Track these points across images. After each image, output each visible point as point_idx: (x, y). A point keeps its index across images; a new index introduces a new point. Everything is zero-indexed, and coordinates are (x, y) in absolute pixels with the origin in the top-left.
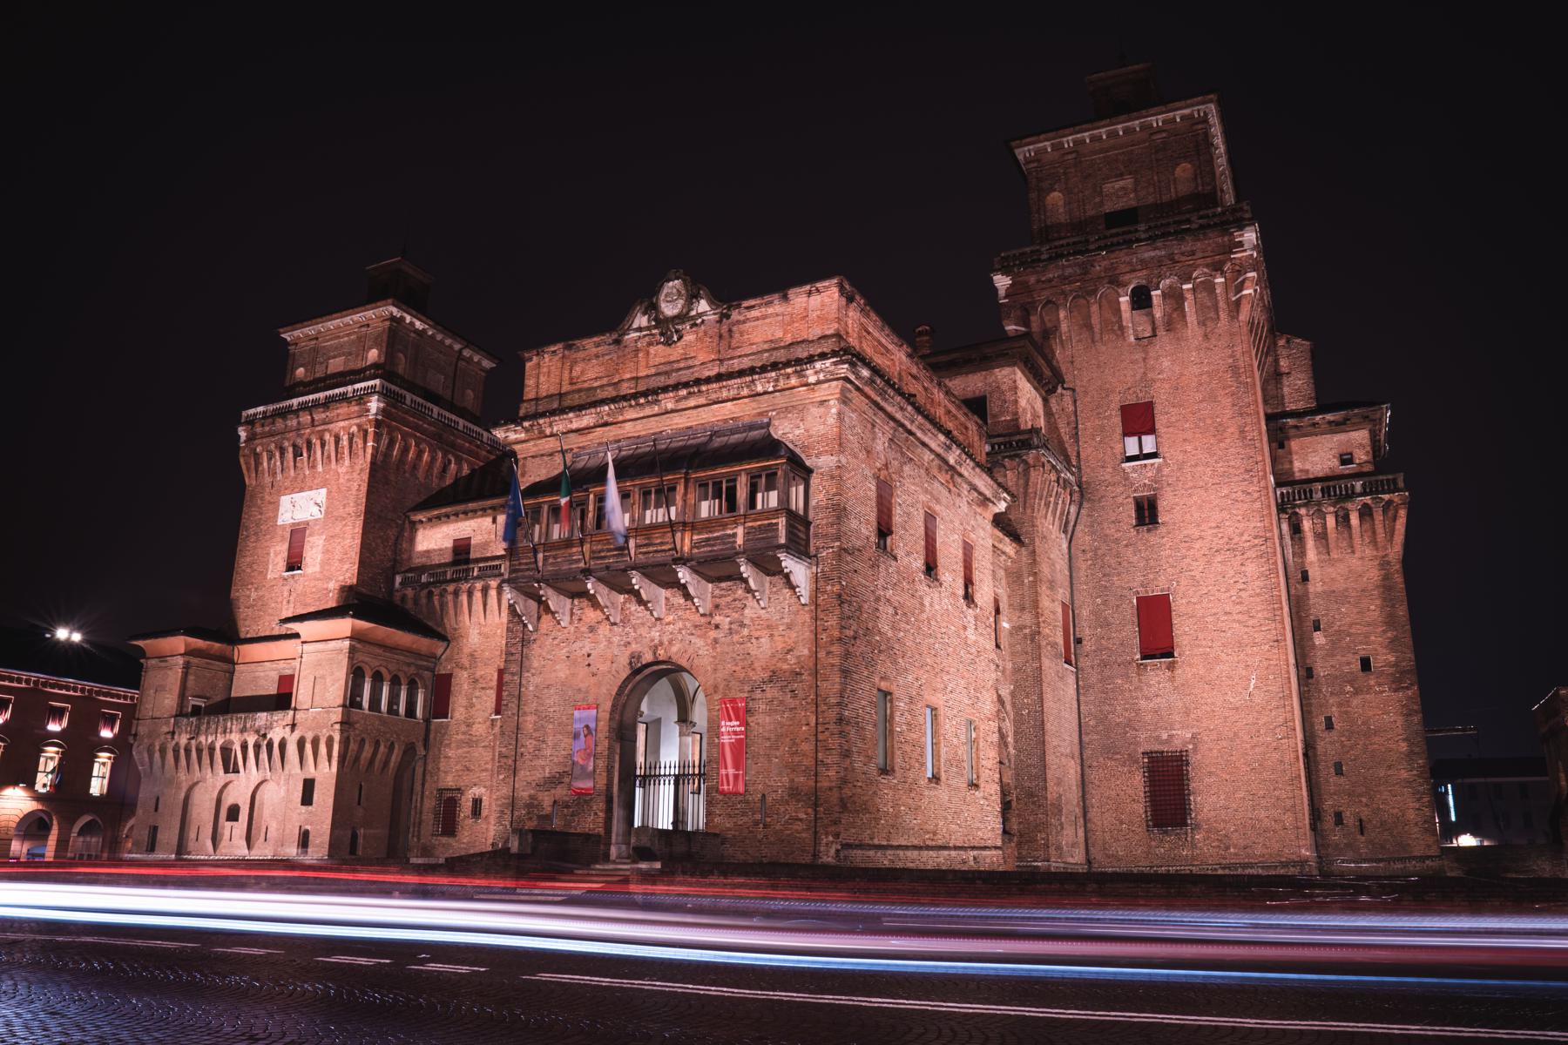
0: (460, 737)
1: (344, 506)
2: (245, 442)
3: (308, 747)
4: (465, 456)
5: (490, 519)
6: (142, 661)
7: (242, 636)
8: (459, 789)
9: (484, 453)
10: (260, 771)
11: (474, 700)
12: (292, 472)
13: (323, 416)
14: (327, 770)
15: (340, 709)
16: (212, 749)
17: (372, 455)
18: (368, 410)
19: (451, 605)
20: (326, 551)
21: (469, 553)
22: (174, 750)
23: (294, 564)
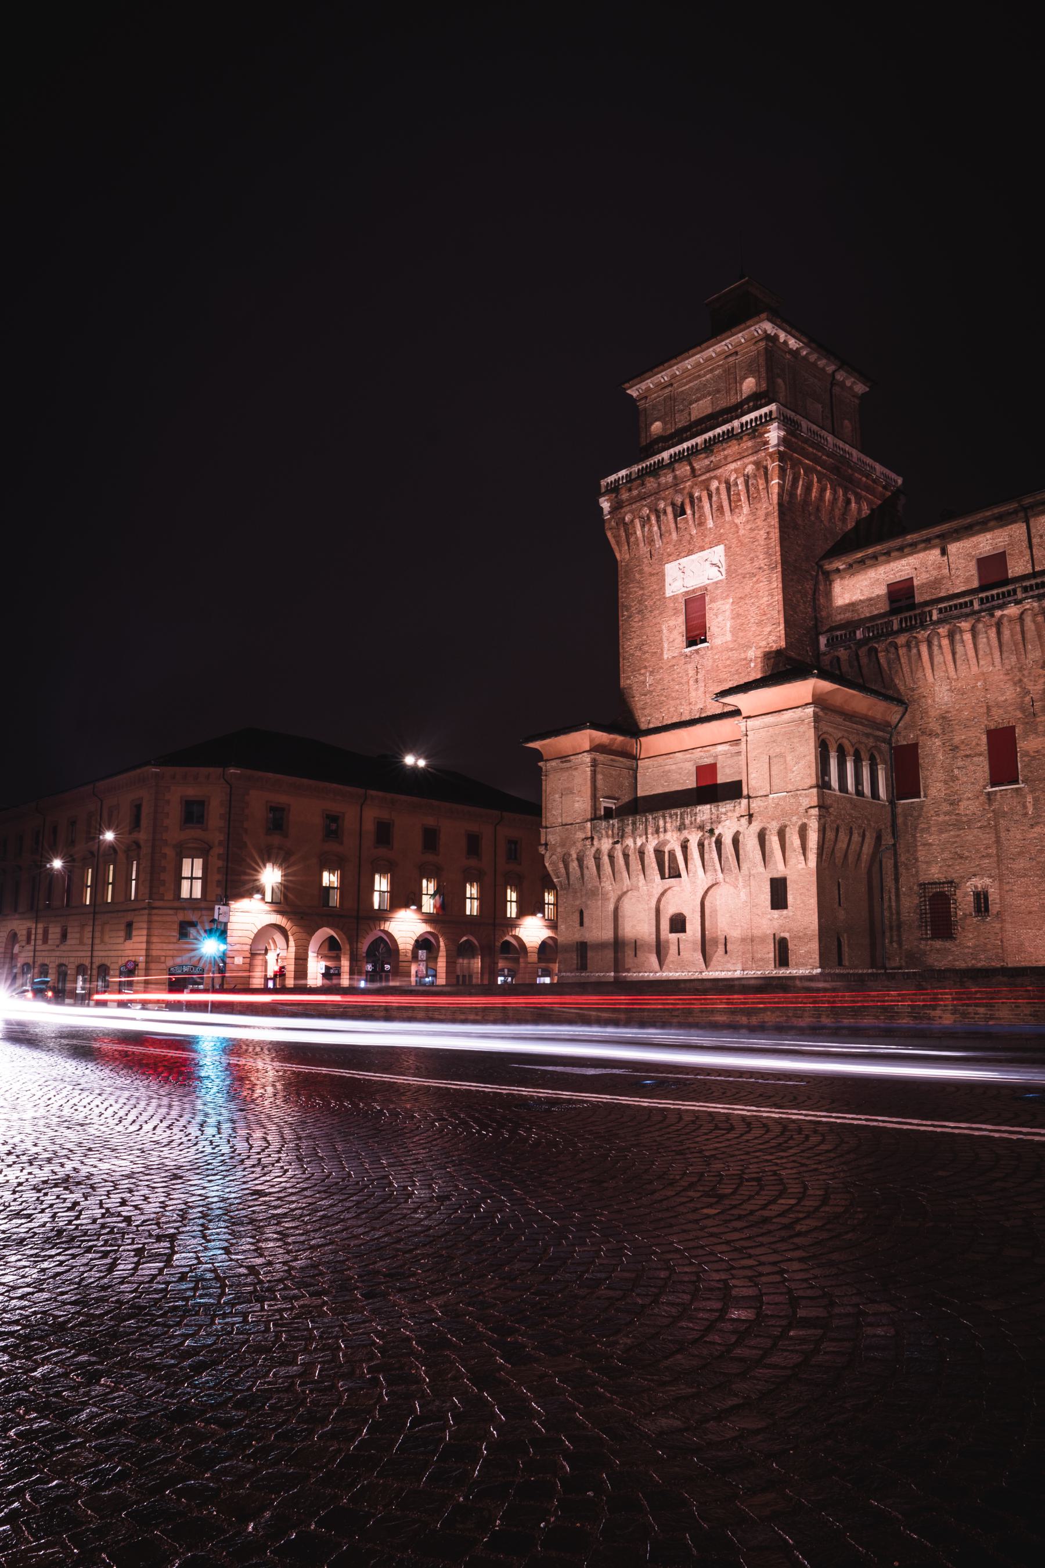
0: (941, 818)
1: (752, 560)
2: (610, 513)
3: (774, 841)
4: (864, 493)
5: (937, 552)
6: (541, 764)
7: (643, 726)
8: (951, 882)
9: (880, 489)
10: (708, 874)
11: (956, 771)
12: (674, 536)
13: (707, 462)
14: (802, 865)
15: (815, 790)
16: (641, 853)
17: (779, 494)
18: (766, 443)
19: (904, 660)
20: (736, 616)
21: (913, 597)
22: (595, 858)
23: (696, 635)
